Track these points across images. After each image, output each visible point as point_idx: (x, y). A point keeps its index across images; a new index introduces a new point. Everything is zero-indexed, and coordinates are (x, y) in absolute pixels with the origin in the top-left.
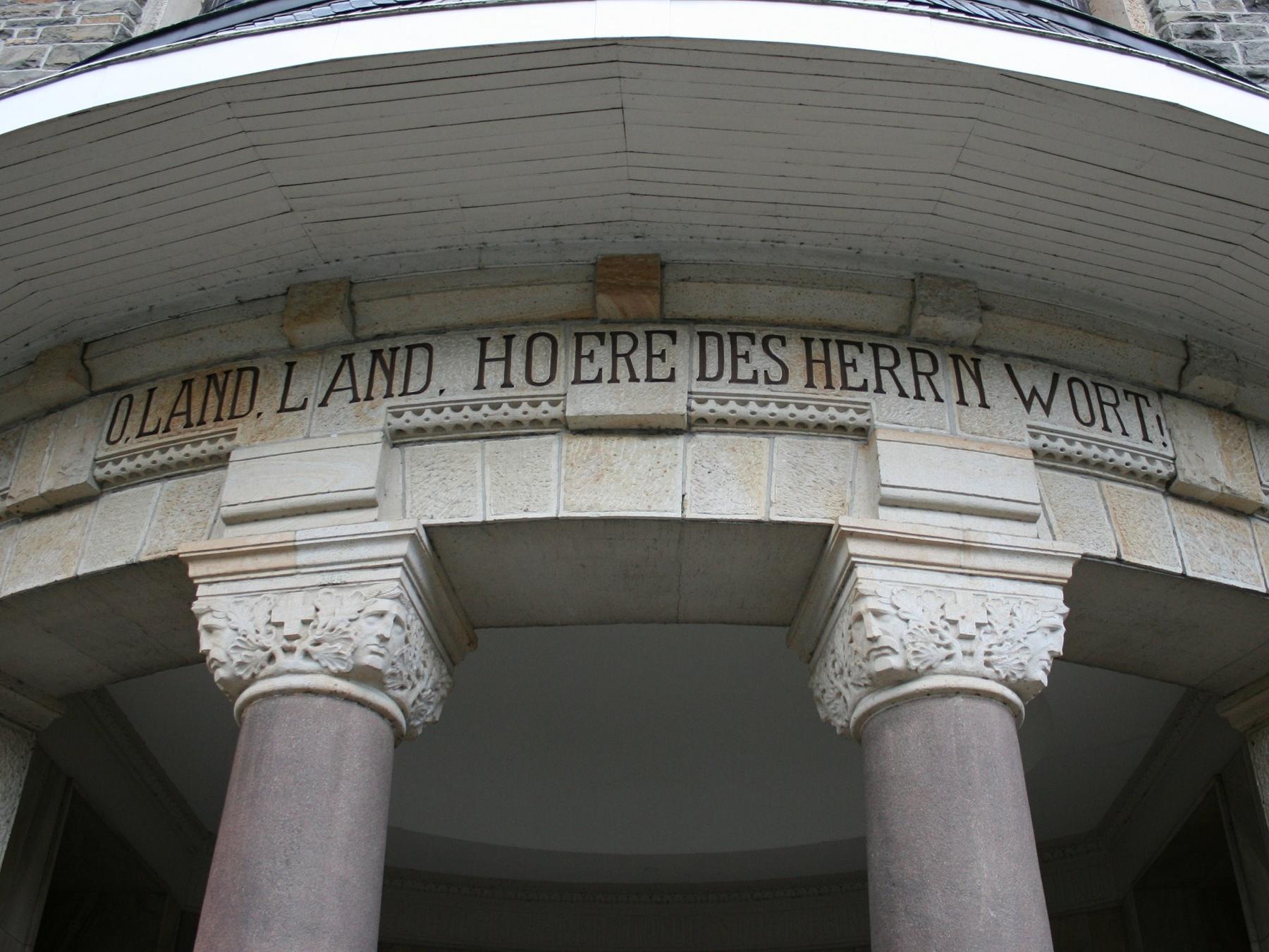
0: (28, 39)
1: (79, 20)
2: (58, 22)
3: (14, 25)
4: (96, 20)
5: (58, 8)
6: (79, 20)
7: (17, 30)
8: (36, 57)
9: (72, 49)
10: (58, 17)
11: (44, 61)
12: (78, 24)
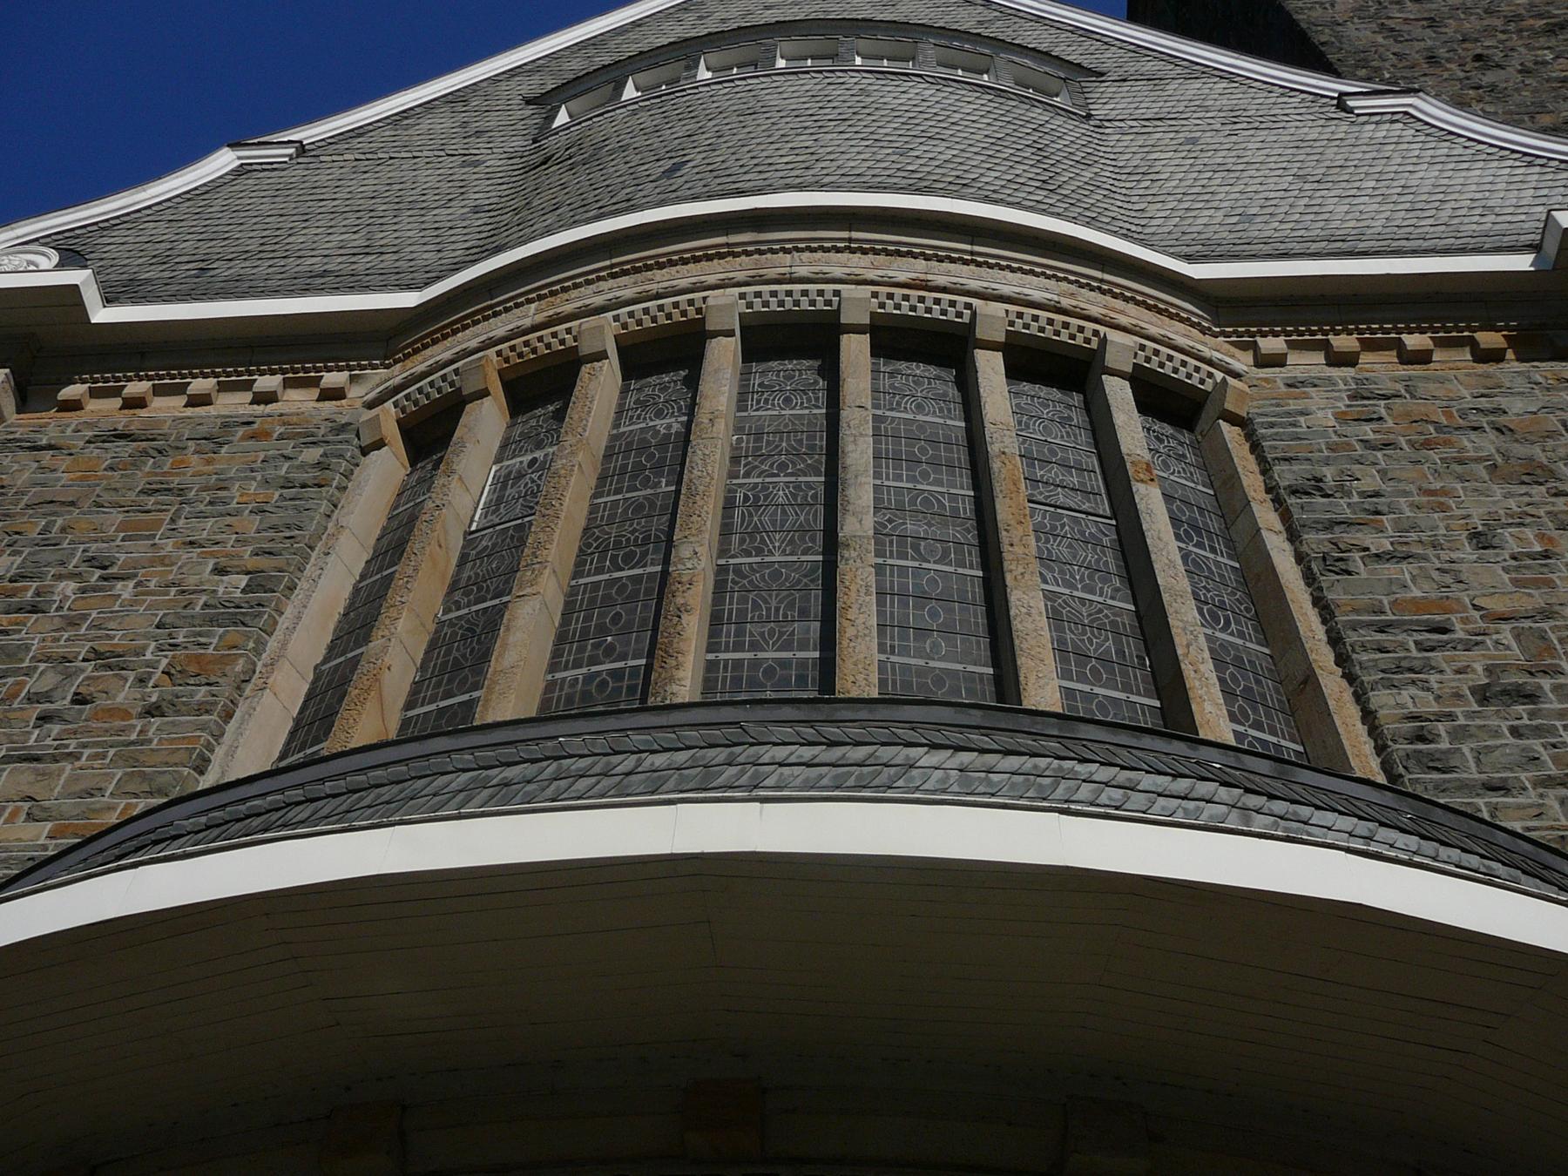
0: (97, 763)
2: (132, 743)
3: (85, 746)
5: (134, 726)
7: (87, 752)
10: (134, 737)
11: (111, 788)
12: (153, 746)
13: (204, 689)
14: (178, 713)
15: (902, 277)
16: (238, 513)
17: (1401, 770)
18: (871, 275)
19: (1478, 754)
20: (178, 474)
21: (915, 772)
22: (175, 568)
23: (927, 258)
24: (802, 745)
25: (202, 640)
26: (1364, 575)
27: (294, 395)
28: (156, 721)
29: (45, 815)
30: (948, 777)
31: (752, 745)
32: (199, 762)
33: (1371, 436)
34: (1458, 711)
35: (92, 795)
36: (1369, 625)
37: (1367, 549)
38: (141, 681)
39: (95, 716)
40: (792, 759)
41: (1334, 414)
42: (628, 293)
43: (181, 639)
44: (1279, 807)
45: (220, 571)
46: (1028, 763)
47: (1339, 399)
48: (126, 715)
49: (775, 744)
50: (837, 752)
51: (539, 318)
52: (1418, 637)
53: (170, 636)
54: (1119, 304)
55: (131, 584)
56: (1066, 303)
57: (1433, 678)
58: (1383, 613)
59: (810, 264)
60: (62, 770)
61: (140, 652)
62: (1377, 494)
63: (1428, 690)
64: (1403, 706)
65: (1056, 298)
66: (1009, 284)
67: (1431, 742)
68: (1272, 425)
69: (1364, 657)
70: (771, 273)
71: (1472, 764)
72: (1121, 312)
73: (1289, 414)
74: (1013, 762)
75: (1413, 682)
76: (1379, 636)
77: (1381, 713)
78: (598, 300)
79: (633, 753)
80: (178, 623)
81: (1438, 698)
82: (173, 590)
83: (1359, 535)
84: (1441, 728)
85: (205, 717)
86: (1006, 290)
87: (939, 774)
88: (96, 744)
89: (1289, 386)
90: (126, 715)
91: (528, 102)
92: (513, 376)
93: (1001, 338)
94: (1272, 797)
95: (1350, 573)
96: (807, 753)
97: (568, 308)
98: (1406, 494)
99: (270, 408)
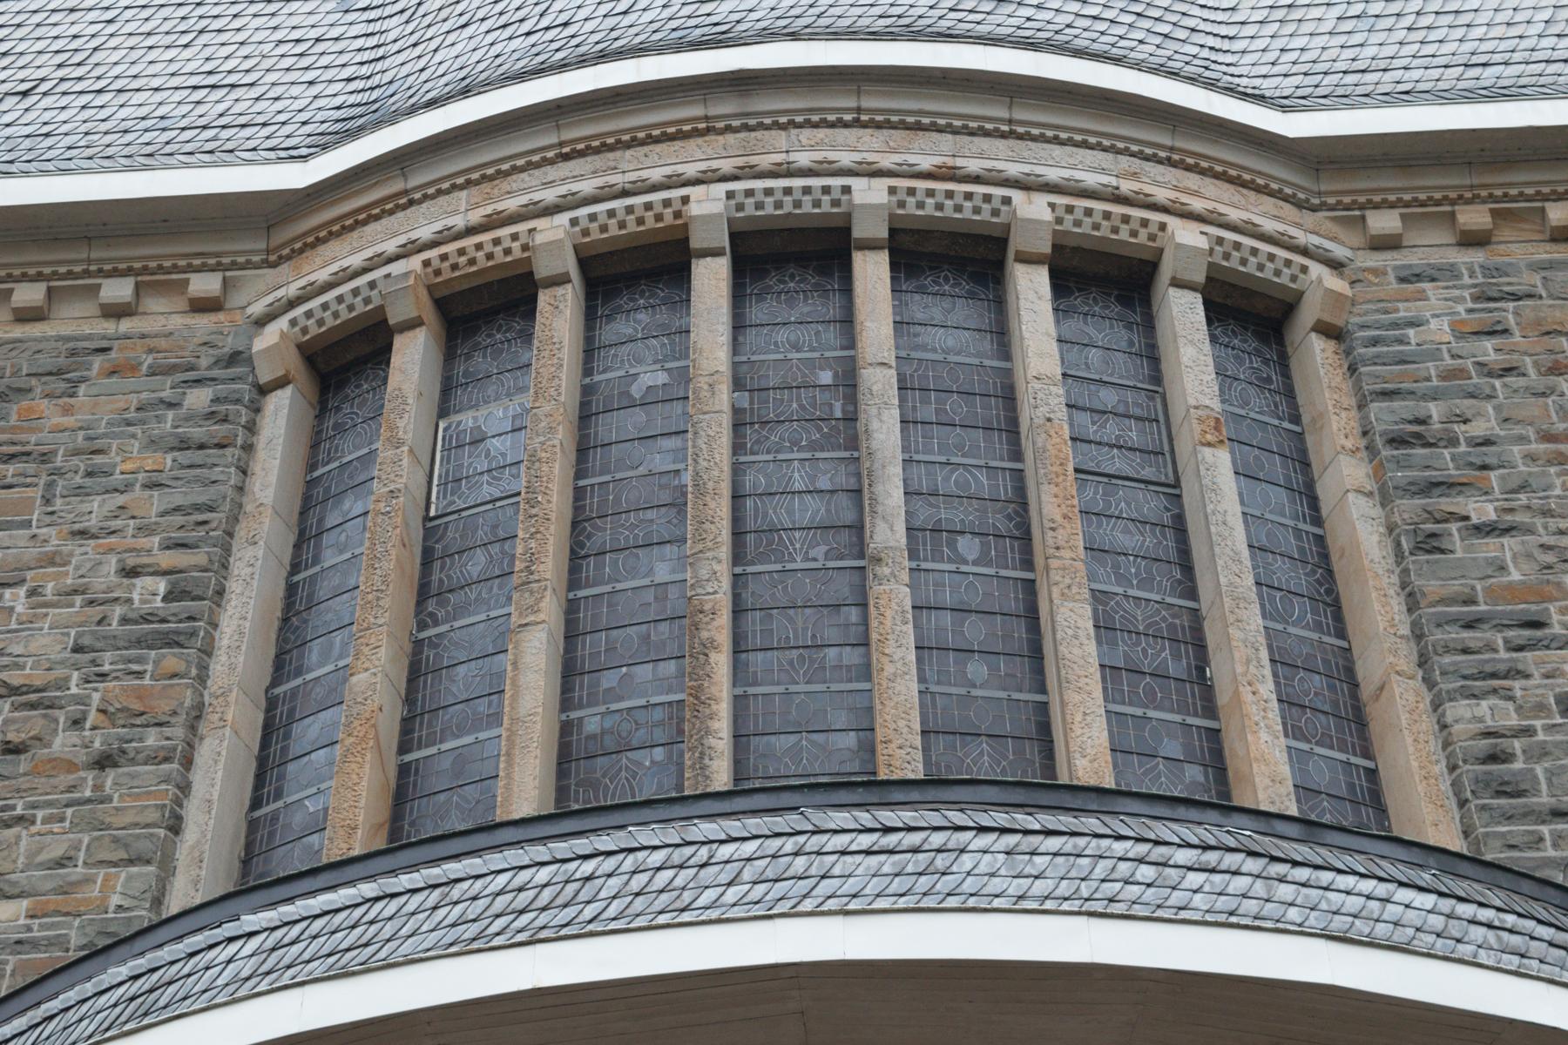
0: (56, 827)
1: (116, 796)
2: (89, 801)
3: (34, 806)
4: (138, 797)
6: (116, 796)
7: (40, 814)
8: (72, 853)
9: (116, 840)
10: (88, 793)
11: (82, 856)
12: (115, 804)
13: (153, 731)
14: (133, 762)
15: (926, 163)
16: (126, 488)
17: (1469, 795)
18: (887, 161)
19: (1550, 775)
20: (32, 430)
21: (965, 857)
22: (70, 568)
23: (955, 132)
24: (860, 831)
25: (135, 667)
26: (1459, 555)
27: (154, 304)
28: (110, 776)
29: (17, 891)
30: (996, 860)
31: (814, 833)
32: (171, 822)
33: (1492, 356)
34: (1538, 723)
35: (63, 866)
36: (1452, 621)
37: (1467, 518)
38: (76, 722)
39: (33, 772)
40: (853, 848)
41: (1452, 325)
42: (587, 187)
43: (107, 668)
44: (1302, 874)
45: (132, 573)
46: (1069, 844)
47: (1459, 300)
48: (71, 767)
49: (835, 832)
50: (891, 840)
51: (475, 217)
52: (1511, 633)
53: (94, 662)
54: (1192, 181)
55: (22, 591)
56: (1126, 187)
57: (1517, 685)
58: (1474, 602)
59: (812, 148)
60: (18, 838)
61: (62, 684)
62: (1488, 442)
63: (1511, 698)
64: (1481, 720)
65: (1114, 181)
66: (1057, 165)
67: (1504, 762)
68: (1375, 342)
69: (1447, 659)
70: (765, 161)
71: (1544, 787)
72: (1195, 193)
73: (1395, 325)
74: (1053, 843)
75: (1495, 691)
76: (1466, 634)
77: (1457, 728)
78: (549, 196)
79: (704, 843)
80: (99, 645)
81: (1519, 709)
82: (78, 600)
83: (1460, 499)
84: (1517, 745)
85: (165, 767)
86: (1053, 175)
87: (988, 857)
88: (49, 804)
89: (1402, 280)
90: (71, 767)
92: (446, 292)
93: (1046, 248)
94: (1295, 864)
95: (1443, 551)
96: (865, 841)
97: (511, 204)
98: (1522, 439)
99: (126, 325)
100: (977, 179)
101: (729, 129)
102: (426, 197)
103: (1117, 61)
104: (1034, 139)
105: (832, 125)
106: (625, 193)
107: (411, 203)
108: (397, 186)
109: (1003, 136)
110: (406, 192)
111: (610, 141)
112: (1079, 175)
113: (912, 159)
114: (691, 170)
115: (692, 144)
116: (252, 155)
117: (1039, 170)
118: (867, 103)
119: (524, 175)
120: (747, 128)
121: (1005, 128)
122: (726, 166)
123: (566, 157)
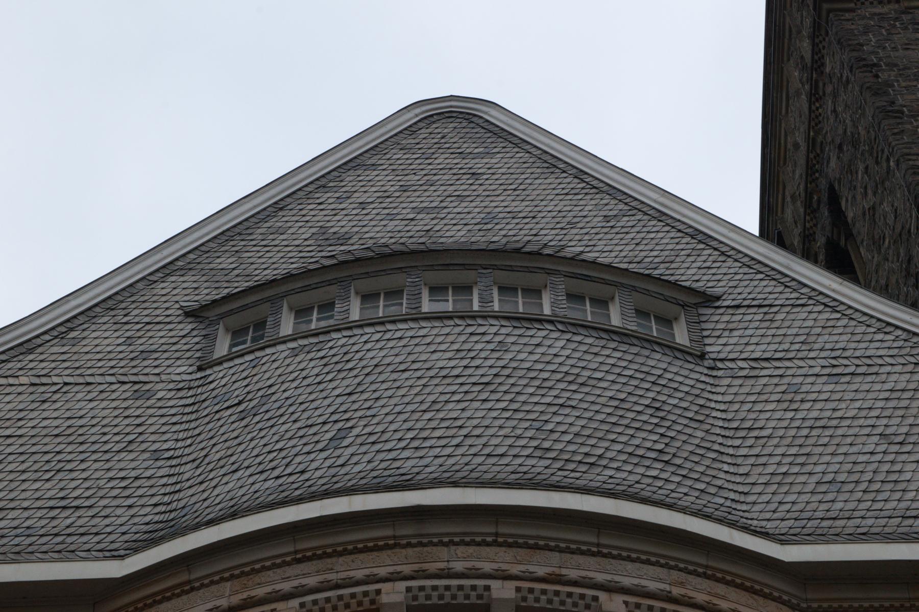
15: (541, 571)
18: (515, 570)
23: (561, 551)
42: (312, 581)
54: (721, 589)
56: (676, 591)
59: (465, 559)
65: (668, 588)
70: (433, 567)
72: (723, 598)
78: (286, 586)
86: (627, 582)
91: (187, 314)
97: (260, 592)
100: (575, 583)
101: (409, 545)
102: (203, 586)
103: (670, 507)
104: (614, 557)
105: (479, 544)
106: (337, 586)
107: (193, 589)
108: (184, 577)
109: (594, 554)
110: (189, 582)
111: (329, 550)
112: (644, 583)
113: (532, 568)
114: (383, 572)
115: (384, 554)
116: (89, 555)
117: (617, 578)
118: (503, 530)
119: (270, 573)
120: (421, 544)
121: (595, 549)
122: (407, 569)
123: (299, 561)
